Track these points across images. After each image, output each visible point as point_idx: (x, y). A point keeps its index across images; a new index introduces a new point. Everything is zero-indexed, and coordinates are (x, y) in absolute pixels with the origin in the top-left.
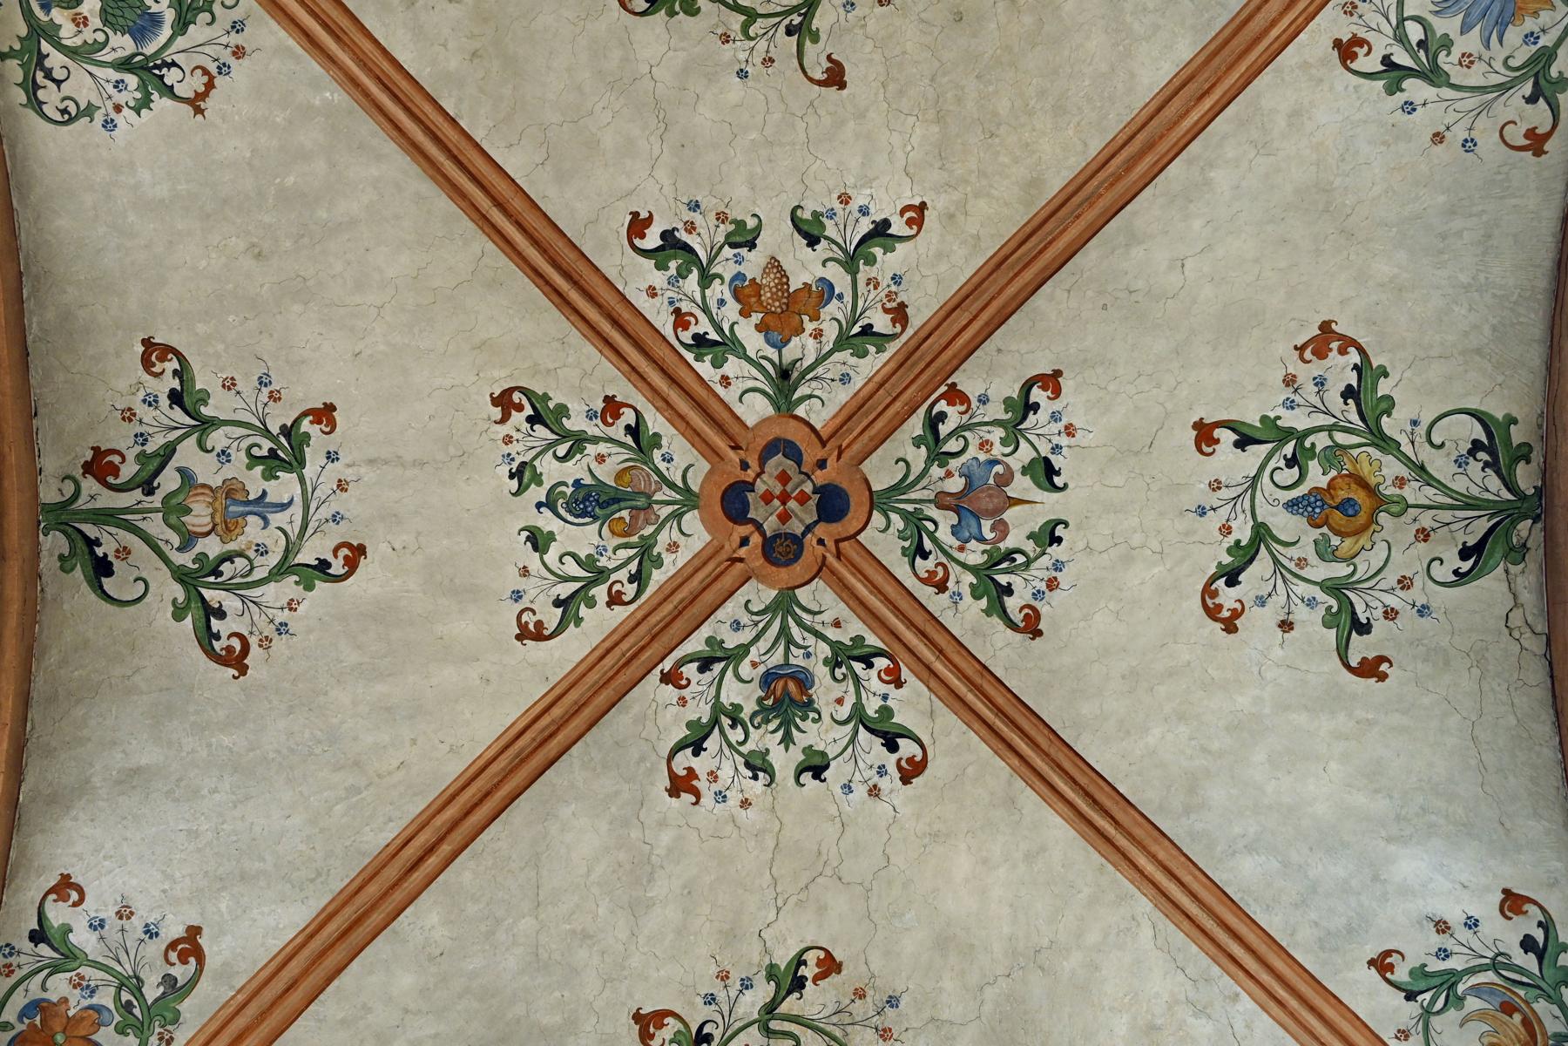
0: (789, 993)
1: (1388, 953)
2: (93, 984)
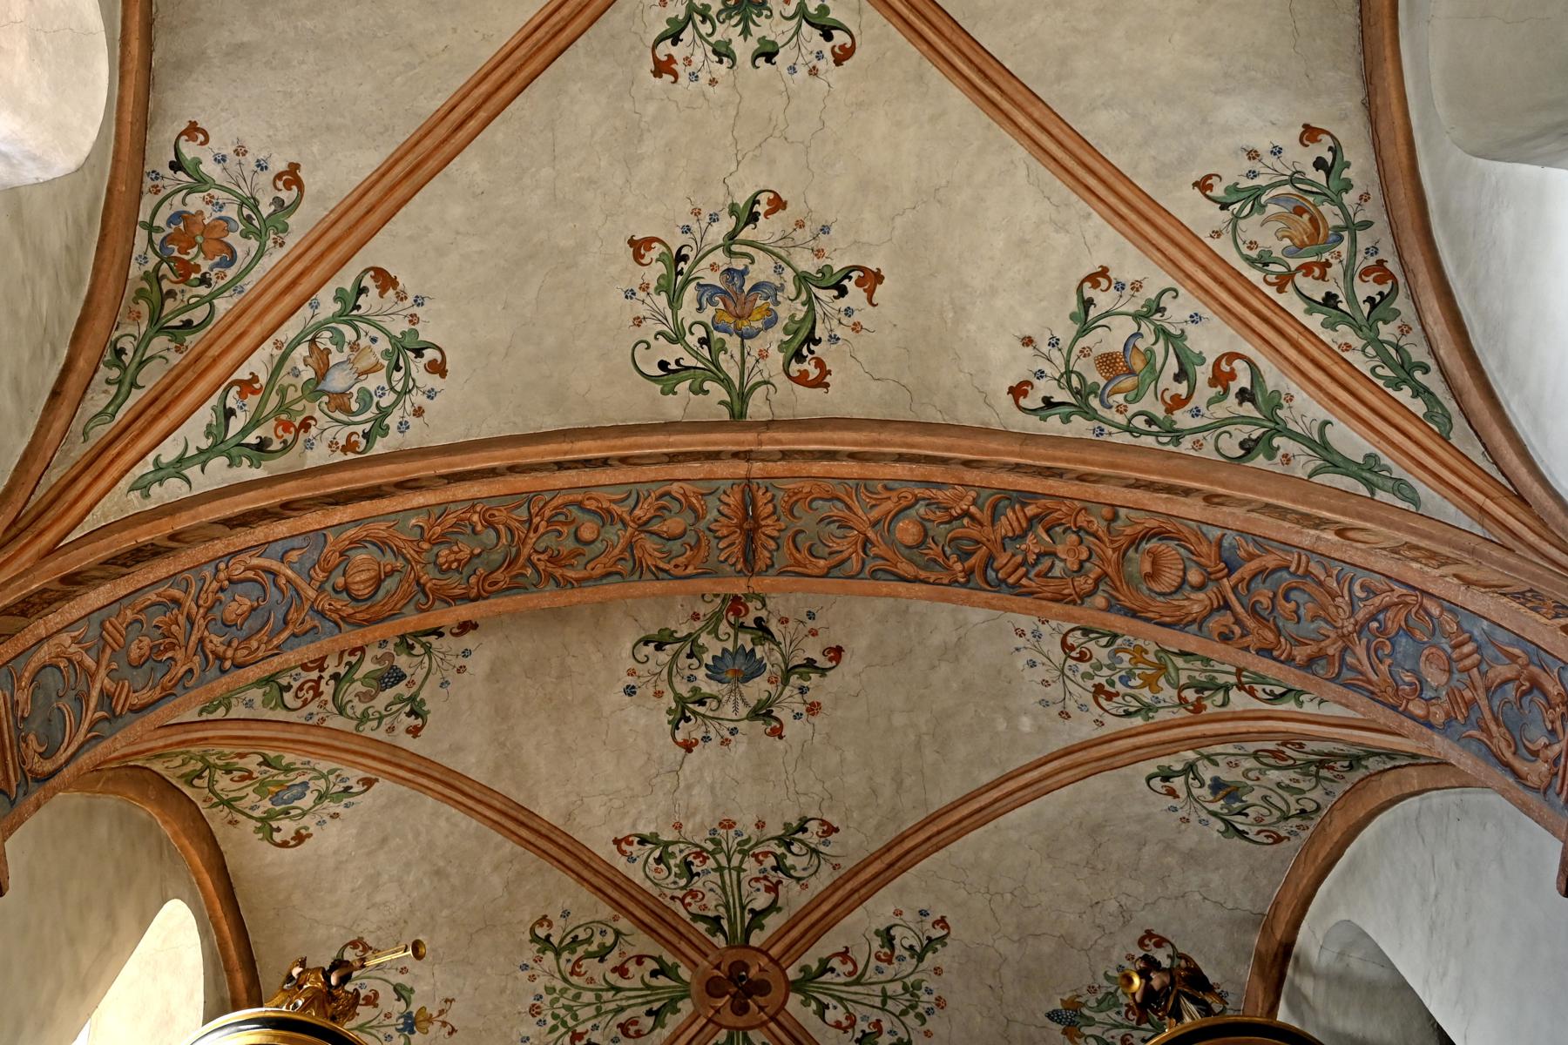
0: (746, 224)
1: (1209, 177)
2: (221, 202)
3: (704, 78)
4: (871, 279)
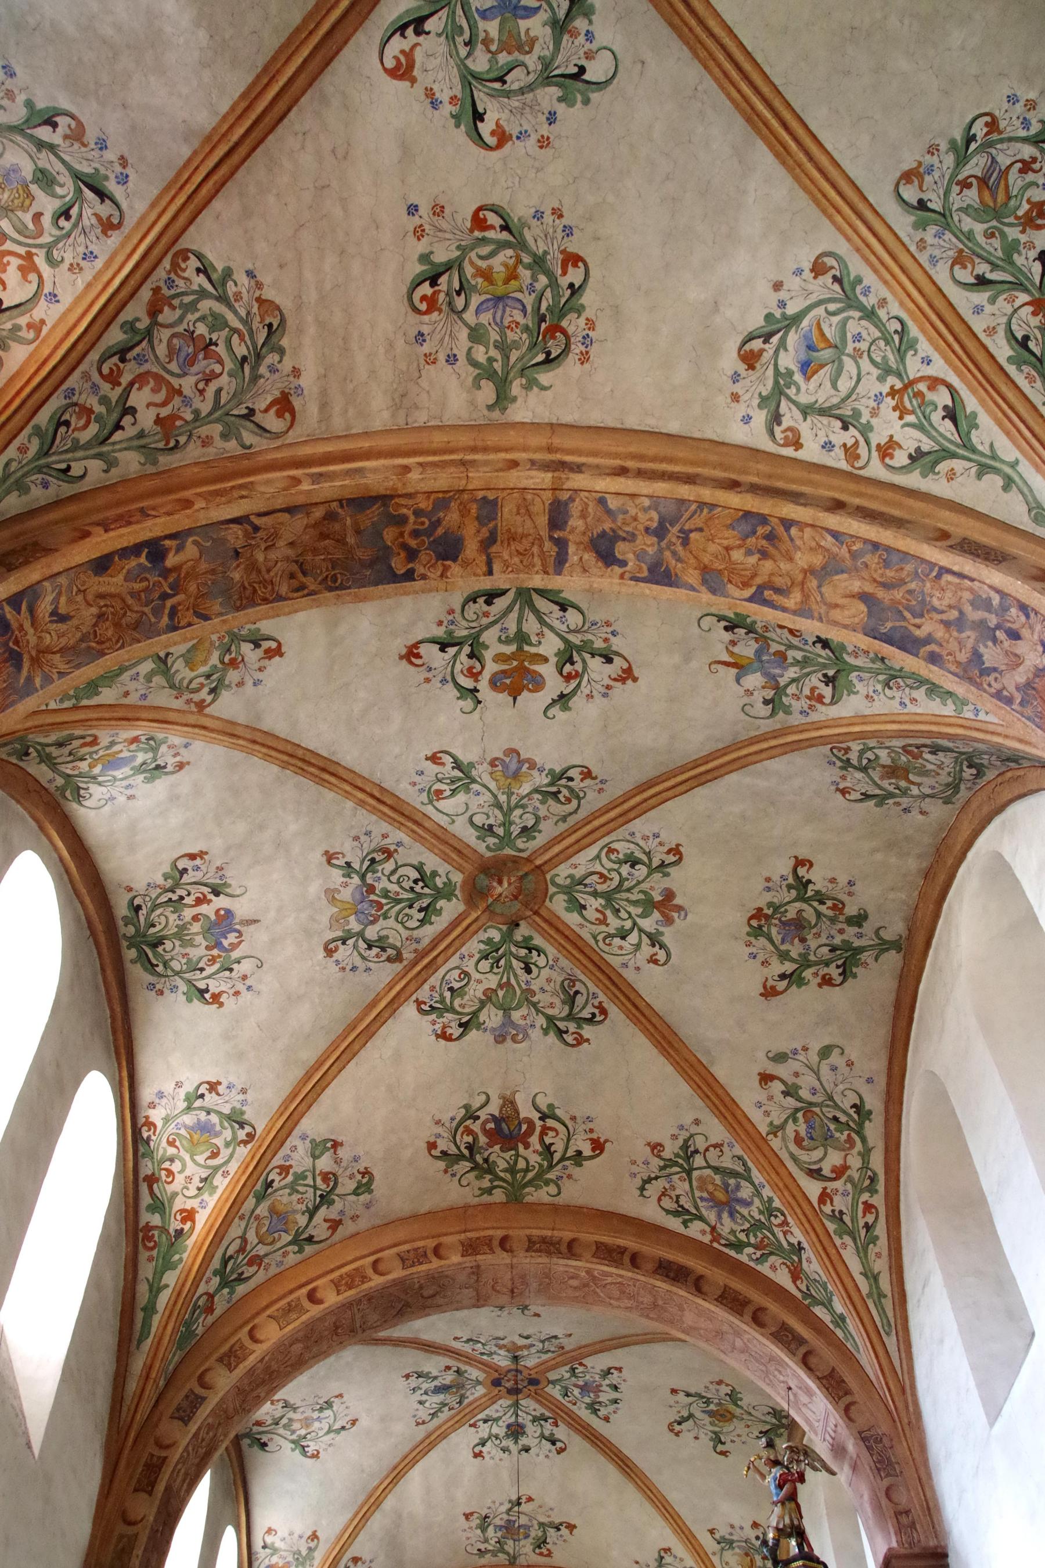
3: (497, 1458)
4: (571, 1527)
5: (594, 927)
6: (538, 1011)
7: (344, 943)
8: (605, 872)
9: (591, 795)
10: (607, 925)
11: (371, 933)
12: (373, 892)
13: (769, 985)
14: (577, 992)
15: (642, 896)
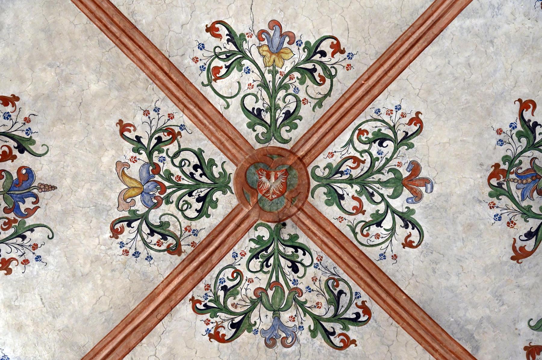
5: (351, 218)
6: (305, 312)
7: (129, 225)
8: (358, 155)
9: (341, 72)
10: (363, 212)
11: (154, 217)
12: (158, 174)
13: (518, 246)
14: (341, 292)
15: (391, 175)
